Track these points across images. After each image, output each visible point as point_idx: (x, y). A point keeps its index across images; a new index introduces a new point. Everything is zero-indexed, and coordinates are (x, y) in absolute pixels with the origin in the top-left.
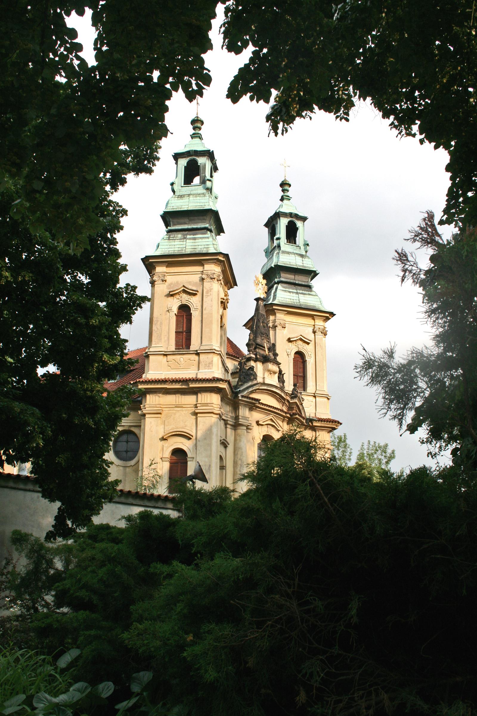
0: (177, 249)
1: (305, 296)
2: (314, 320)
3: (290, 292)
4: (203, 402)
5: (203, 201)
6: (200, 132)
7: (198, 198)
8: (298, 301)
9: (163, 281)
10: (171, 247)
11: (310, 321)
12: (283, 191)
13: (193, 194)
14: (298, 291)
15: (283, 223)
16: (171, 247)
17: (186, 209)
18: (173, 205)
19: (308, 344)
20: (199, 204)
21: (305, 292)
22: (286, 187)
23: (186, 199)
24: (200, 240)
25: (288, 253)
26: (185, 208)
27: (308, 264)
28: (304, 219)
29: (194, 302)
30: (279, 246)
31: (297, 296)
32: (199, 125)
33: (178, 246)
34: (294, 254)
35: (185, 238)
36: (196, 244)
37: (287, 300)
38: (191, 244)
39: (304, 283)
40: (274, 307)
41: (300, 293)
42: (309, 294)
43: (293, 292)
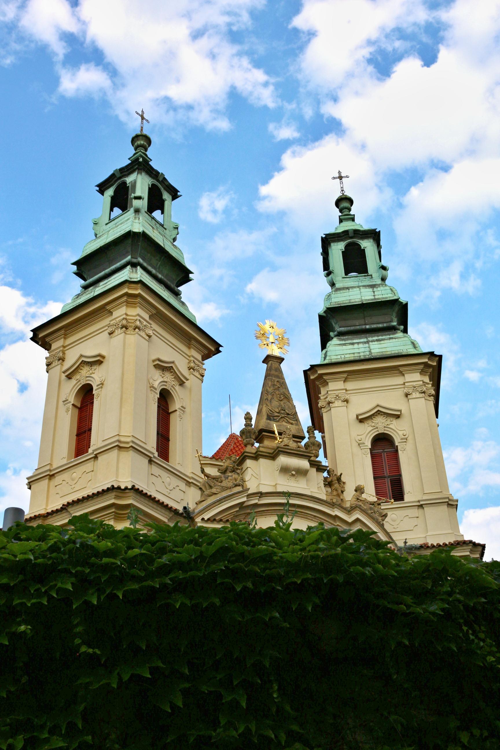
1: (382, 342)
2: (403, 375)
3: (353, 344)
8: (368, 353)
14: (370, 339)
15: (337, 249)
19: (398, 417)
21: (384, 337)
25: (348, 288)
27: (383, 294)
31: (367, 345)
32: (141, 142)
34: (359, 287)
37: (346, 356)
39: (380, 326)
40: (320, 371)
41: (372, 341)
43: (358, 343)
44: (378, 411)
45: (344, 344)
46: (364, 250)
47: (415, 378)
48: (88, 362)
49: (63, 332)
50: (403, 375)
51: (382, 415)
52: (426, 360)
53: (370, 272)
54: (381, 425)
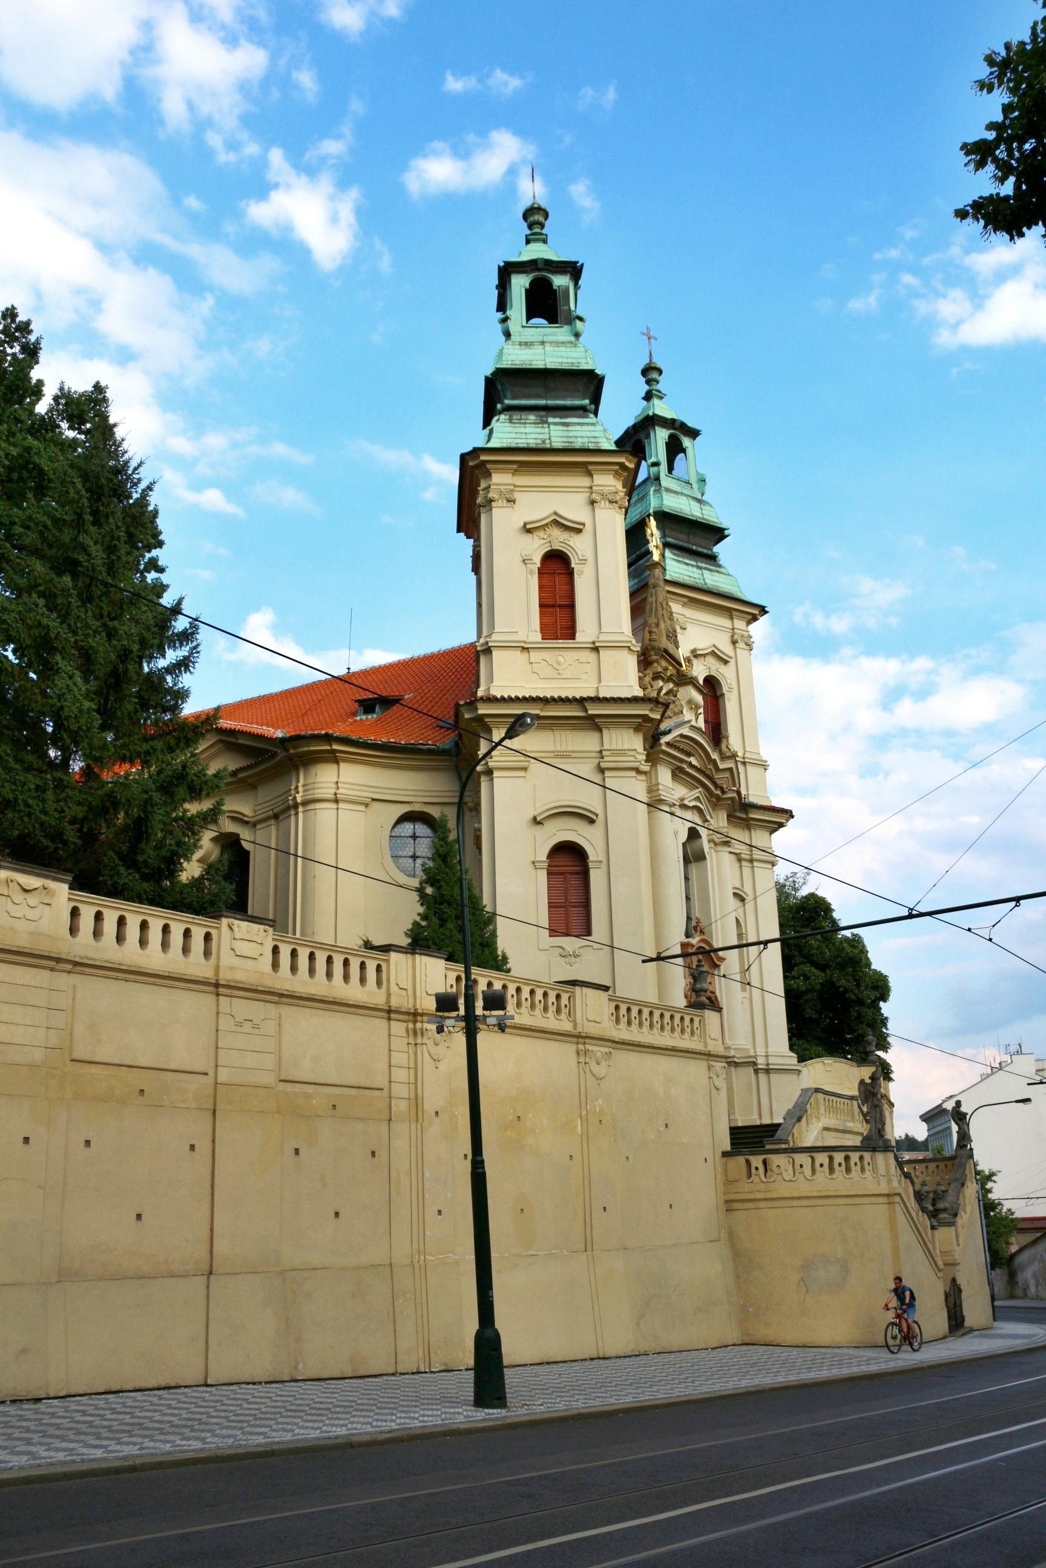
0: (533, 441)
3: (687, 564)
4: (614, 747)
5: (574, 355)
6: (544, 231)
7: (563, 349)
9: (509, 501)
10: (518, 436)
11: (726, 622)
12: (648, 382)
13: (551, 343)
16: (518, 436)
17: (541, 367)
18: (512, 357)
19: (726, 662)
20: (565, 360)
22: (654, 375)
23: (538, 350)
24: (578, 428)
25: (676, 492)
26: (539, 364)
28: (694, 434)
29: (577, 547)
30: (657, 479)
33: (533, 436)
34: (686, 495)
35: (543, 422)
36: (571, 434)
38: (561, 434)
42: (718, 572)
45: (679, 562)
48: (563, 525)
49: (515, 466)
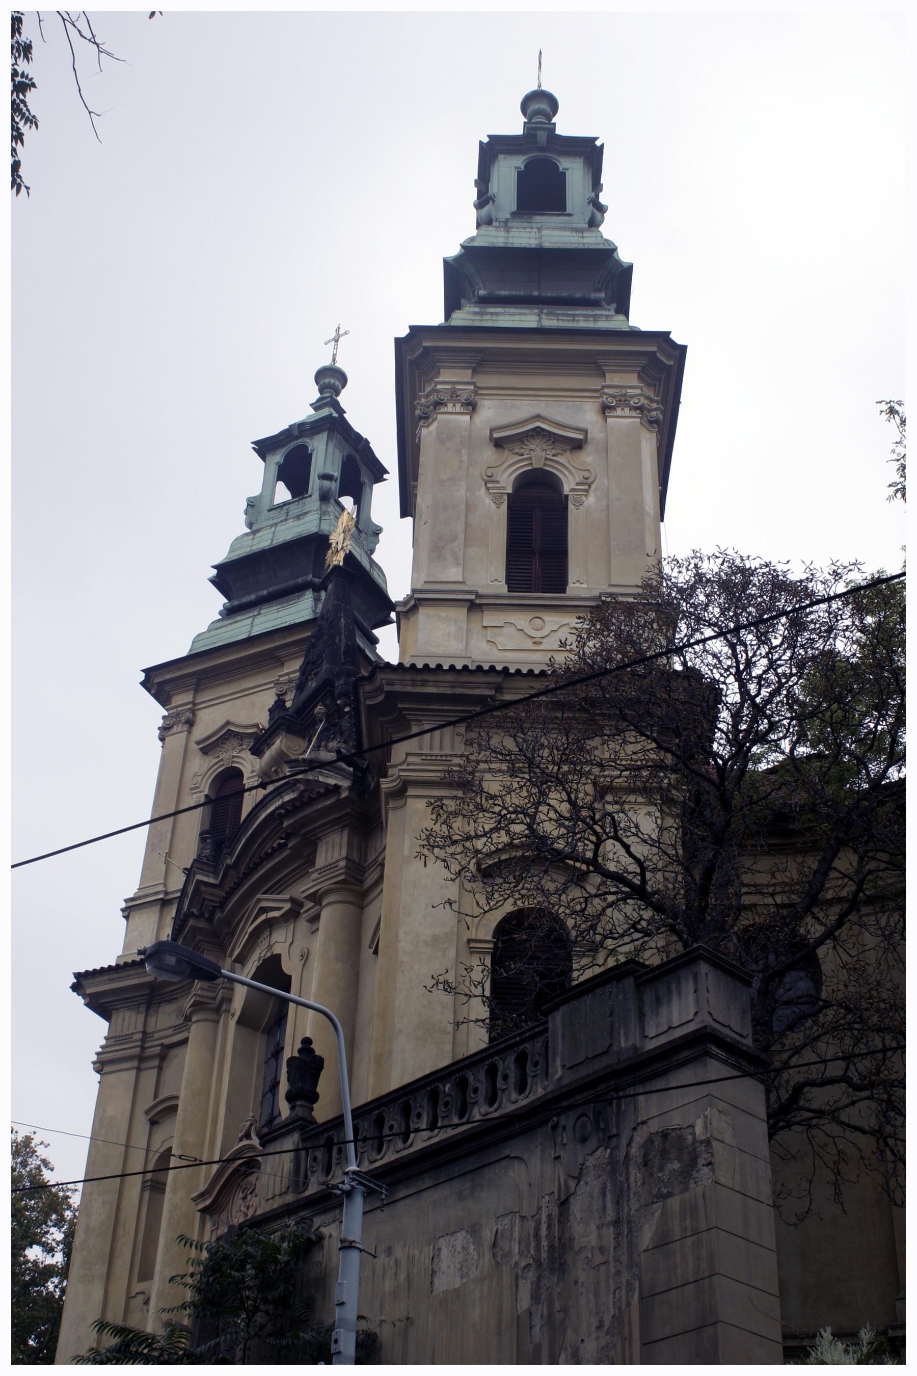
27: (588, 241)
44: (538, 427)
46: (563, 175)
47: (627, 381)
50: (603, 375)
51: (544, 436)
52: (654, 349)
53: (569, 210)
54: (537, 455)
